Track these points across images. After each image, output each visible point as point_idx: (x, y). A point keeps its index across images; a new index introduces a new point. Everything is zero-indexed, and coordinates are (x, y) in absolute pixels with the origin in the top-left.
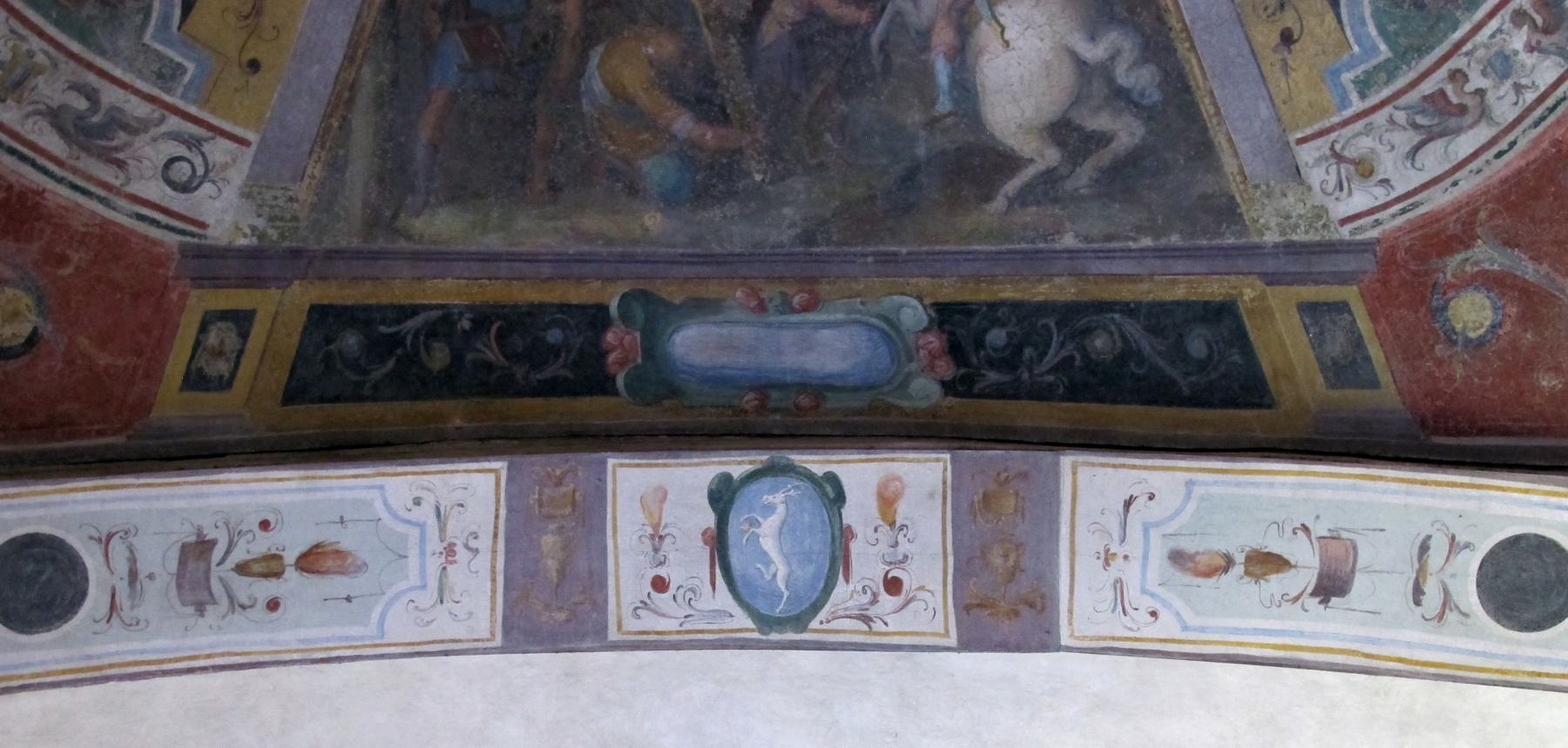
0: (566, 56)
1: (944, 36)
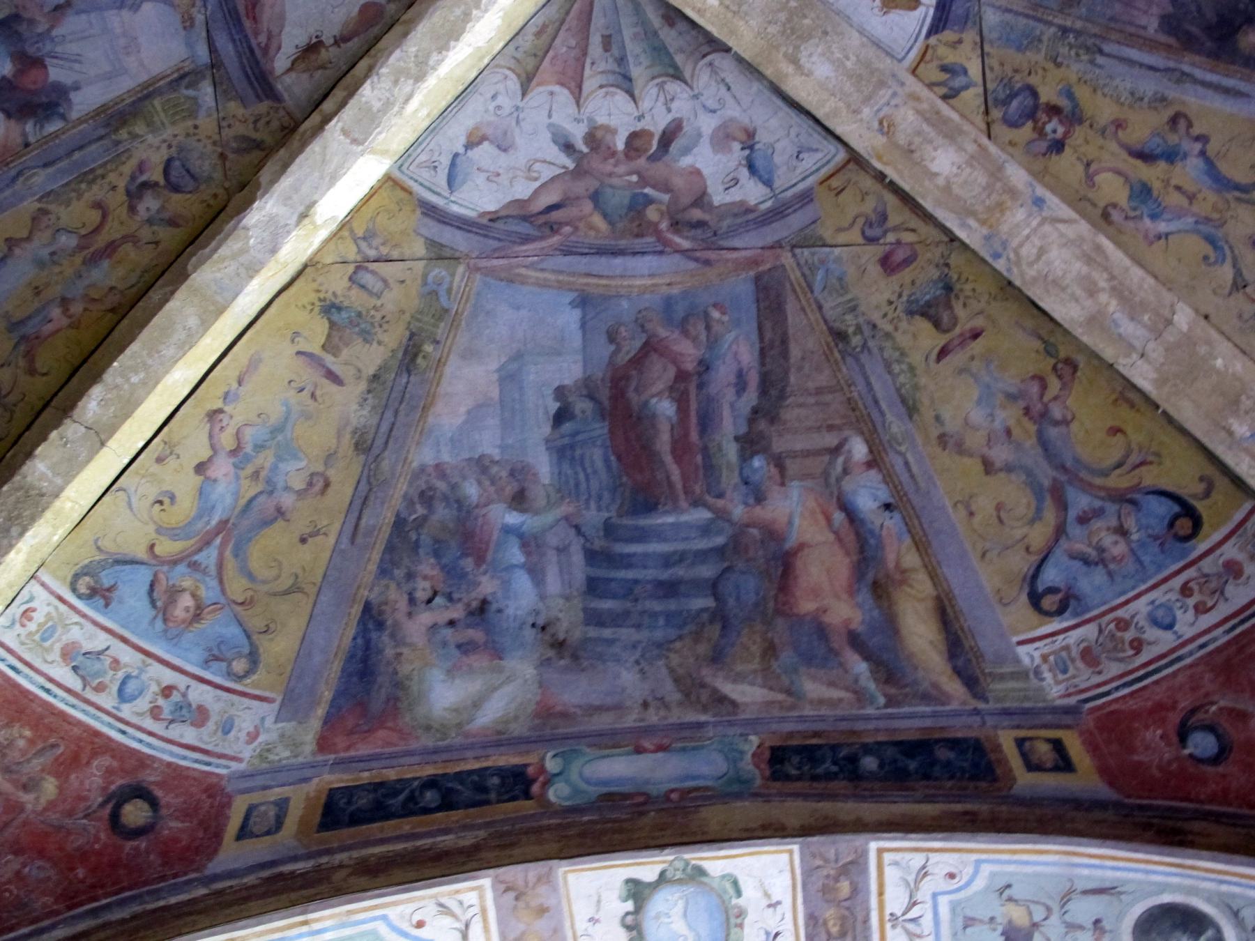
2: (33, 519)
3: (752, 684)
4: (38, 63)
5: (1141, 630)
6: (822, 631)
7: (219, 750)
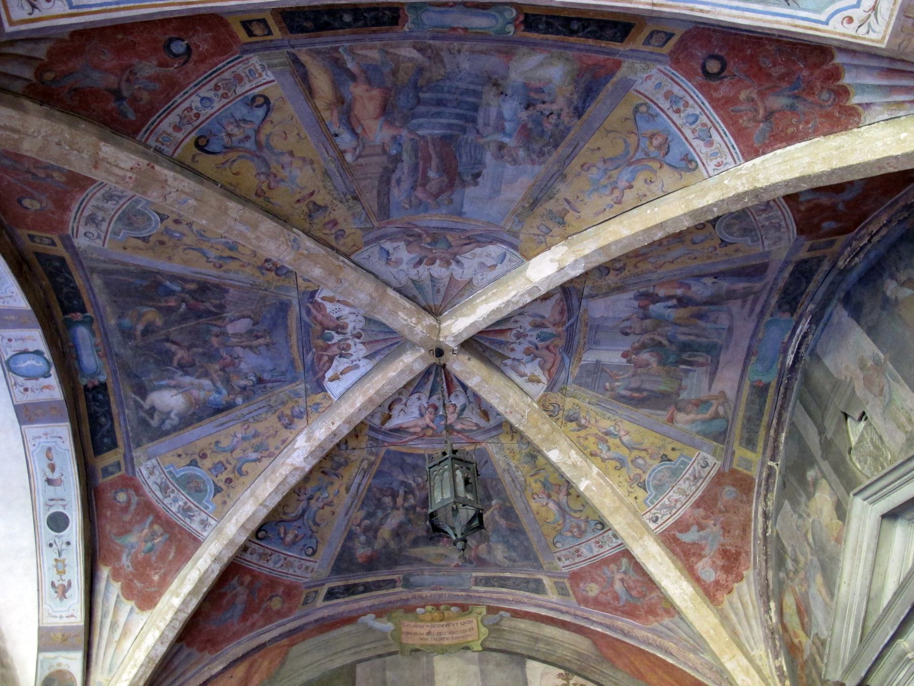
0: (151, 303)
1: (173, 383)
2: (697, 210)
3: (405, 57)
4: (640, 307)
5: (216, 95)
6: (369, 81)
7: (666, 78)
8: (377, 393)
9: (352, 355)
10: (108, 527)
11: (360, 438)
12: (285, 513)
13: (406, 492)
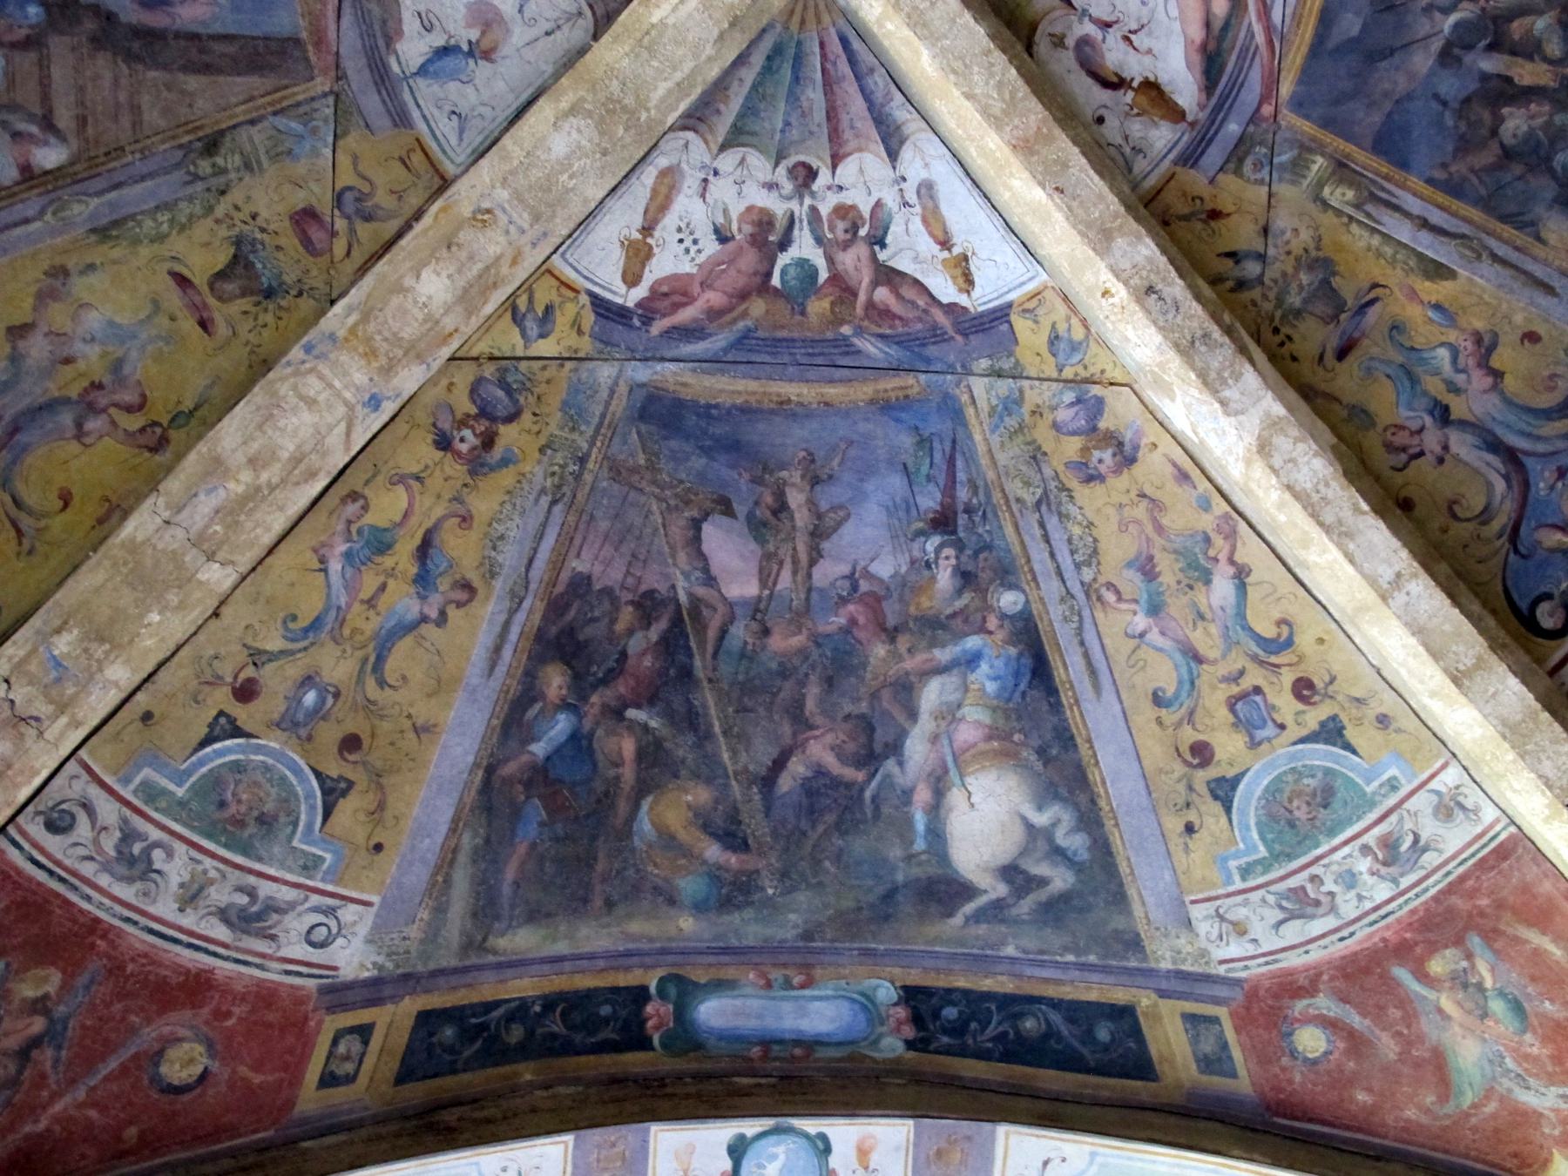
0: (623, 807)
1: (923, 795)
8: (997, 122)
9: (878, 204)
10: (1411, 1113)
11: (1226, 204)
12: (1485, 516)
13: (1492, 47)
